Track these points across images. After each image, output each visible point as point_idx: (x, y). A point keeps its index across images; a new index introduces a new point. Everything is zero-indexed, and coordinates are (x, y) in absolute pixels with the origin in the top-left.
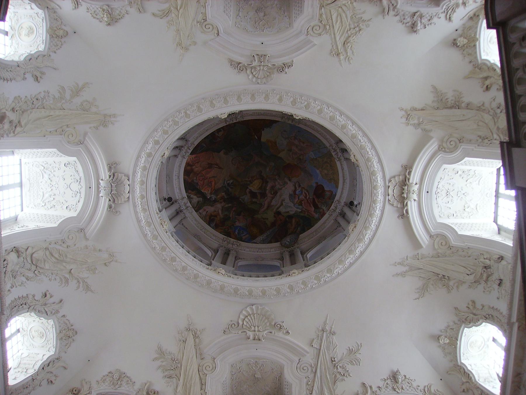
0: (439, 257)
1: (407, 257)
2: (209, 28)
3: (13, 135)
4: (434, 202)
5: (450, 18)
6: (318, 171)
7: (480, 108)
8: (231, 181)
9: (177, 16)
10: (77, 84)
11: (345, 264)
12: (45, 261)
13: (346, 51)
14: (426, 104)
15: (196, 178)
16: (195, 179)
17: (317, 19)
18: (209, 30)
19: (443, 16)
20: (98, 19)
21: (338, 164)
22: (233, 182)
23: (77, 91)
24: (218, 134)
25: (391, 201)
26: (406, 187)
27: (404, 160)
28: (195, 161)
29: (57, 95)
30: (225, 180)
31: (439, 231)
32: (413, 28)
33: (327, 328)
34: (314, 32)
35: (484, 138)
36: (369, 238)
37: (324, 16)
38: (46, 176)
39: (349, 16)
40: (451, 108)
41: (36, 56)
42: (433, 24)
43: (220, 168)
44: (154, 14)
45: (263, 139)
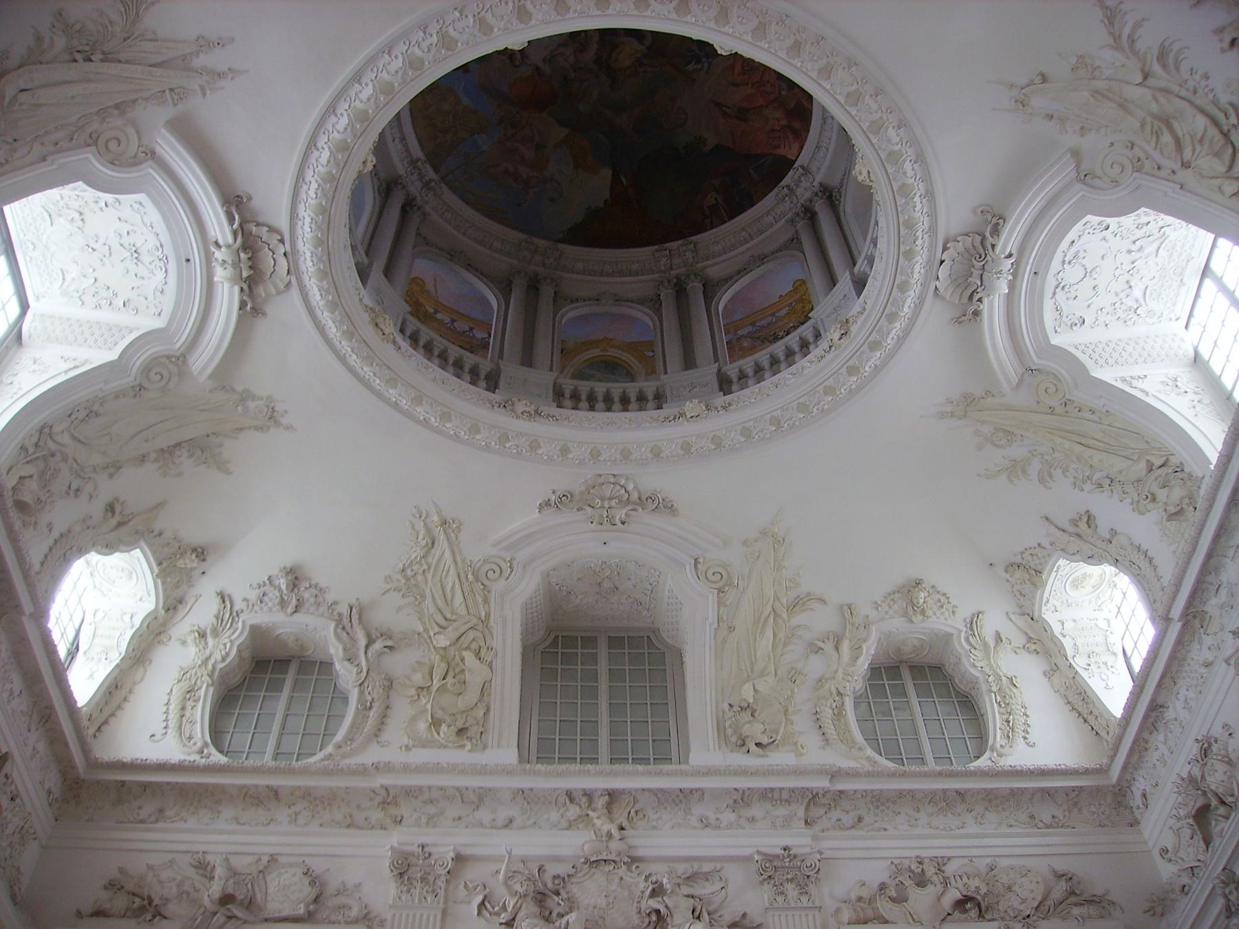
0: (117, 107)
1: (204, 95)
2: (714, 574)
3: (1170, 457)
4: (165, 238)
5: (224, 602)
6: (465, 101)
7: (114, 468)
8: (690, 67)
9: (776, 598)
10: (1011, 481)
11: (375, 82)
12: (1201, 141)
13: (428, 530)
14: (237, 438)
15: (780, 92)
16: (783, 90)
17: (493, 593)
19: (239, 605)
20: (938, 592)
21: (417, 152)
23: (1016, 469)
25: (276, 242)
26: (245, 274)
27: (263, 328)
28: (780, 137)
29: (1057, 473)
31: (134, 174)
32: (295, 576)
35: (92, 414)
37: (480, 600)
38: (1137, 293)
39: (429, 600)
40: (178, 445)
41: (1077, 557)
42: (255, 585)
43: (718, 104)
44: (822, 601)
45: (607, 173)
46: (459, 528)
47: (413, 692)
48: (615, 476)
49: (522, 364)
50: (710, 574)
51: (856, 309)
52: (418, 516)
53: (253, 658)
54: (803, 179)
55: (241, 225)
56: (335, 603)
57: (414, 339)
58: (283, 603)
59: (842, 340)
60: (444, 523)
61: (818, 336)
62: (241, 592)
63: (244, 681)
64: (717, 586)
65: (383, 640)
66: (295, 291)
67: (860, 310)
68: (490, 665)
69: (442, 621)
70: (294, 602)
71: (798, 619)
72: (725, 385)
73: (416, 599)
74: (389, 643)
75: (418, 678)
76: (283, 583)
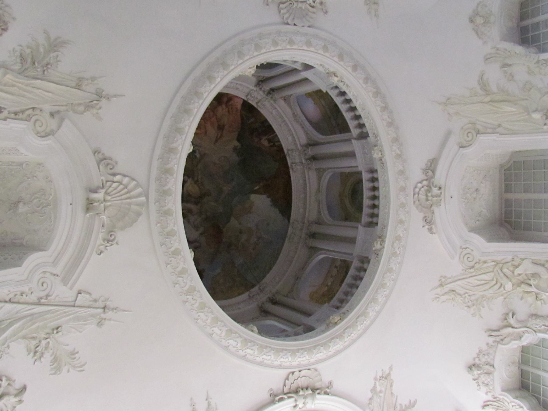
2: (468, 137)
5: (488, 405)
6: (218, 271)
14: (397, 396)
18: (466, 137)
19: (489, 397)
21: (245, 296)
22: (197, 158)
24: (265, 140)
26: (310, 392)
28: (232, 108)
30: (201, 147)
33: (110, 314)
34: (466, 254)
36: (246, 355)
42: (478, 388)
43: (216, 141)
45: (253, 197)
46: (445, 277)
47: (539, 302)
48: (414, 194)
49: (355, 243)
50: (470, 139)
51: (321, 69)
52: (438, 299)
53: (520, 389)
54: (253, 96)
55: (285, 394)
56: (488, 344)
57: (342, 301)
58: (488, 373)
59: (339, 76)
60: (441, 285)
61: (336, 87)
62: (483, 396)
63: (534, 396)
64: (475, 135)
65: (509, 318)
66: (319, 366)
67: (321, 67)
68: (523, 260)
69: (499, 285)
70: (487, 367)
71: (494, 89)
72: (364, 136)
73: (485, 300)
74: (511, 315)
75: (530, 299)
76: (476, 372)
